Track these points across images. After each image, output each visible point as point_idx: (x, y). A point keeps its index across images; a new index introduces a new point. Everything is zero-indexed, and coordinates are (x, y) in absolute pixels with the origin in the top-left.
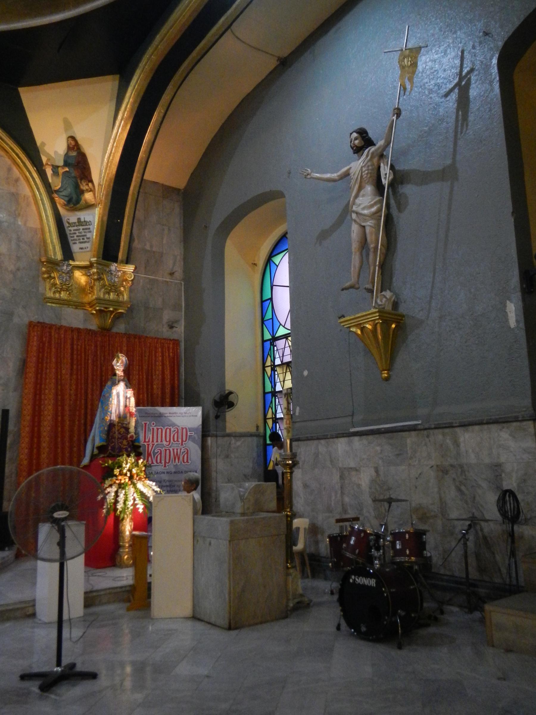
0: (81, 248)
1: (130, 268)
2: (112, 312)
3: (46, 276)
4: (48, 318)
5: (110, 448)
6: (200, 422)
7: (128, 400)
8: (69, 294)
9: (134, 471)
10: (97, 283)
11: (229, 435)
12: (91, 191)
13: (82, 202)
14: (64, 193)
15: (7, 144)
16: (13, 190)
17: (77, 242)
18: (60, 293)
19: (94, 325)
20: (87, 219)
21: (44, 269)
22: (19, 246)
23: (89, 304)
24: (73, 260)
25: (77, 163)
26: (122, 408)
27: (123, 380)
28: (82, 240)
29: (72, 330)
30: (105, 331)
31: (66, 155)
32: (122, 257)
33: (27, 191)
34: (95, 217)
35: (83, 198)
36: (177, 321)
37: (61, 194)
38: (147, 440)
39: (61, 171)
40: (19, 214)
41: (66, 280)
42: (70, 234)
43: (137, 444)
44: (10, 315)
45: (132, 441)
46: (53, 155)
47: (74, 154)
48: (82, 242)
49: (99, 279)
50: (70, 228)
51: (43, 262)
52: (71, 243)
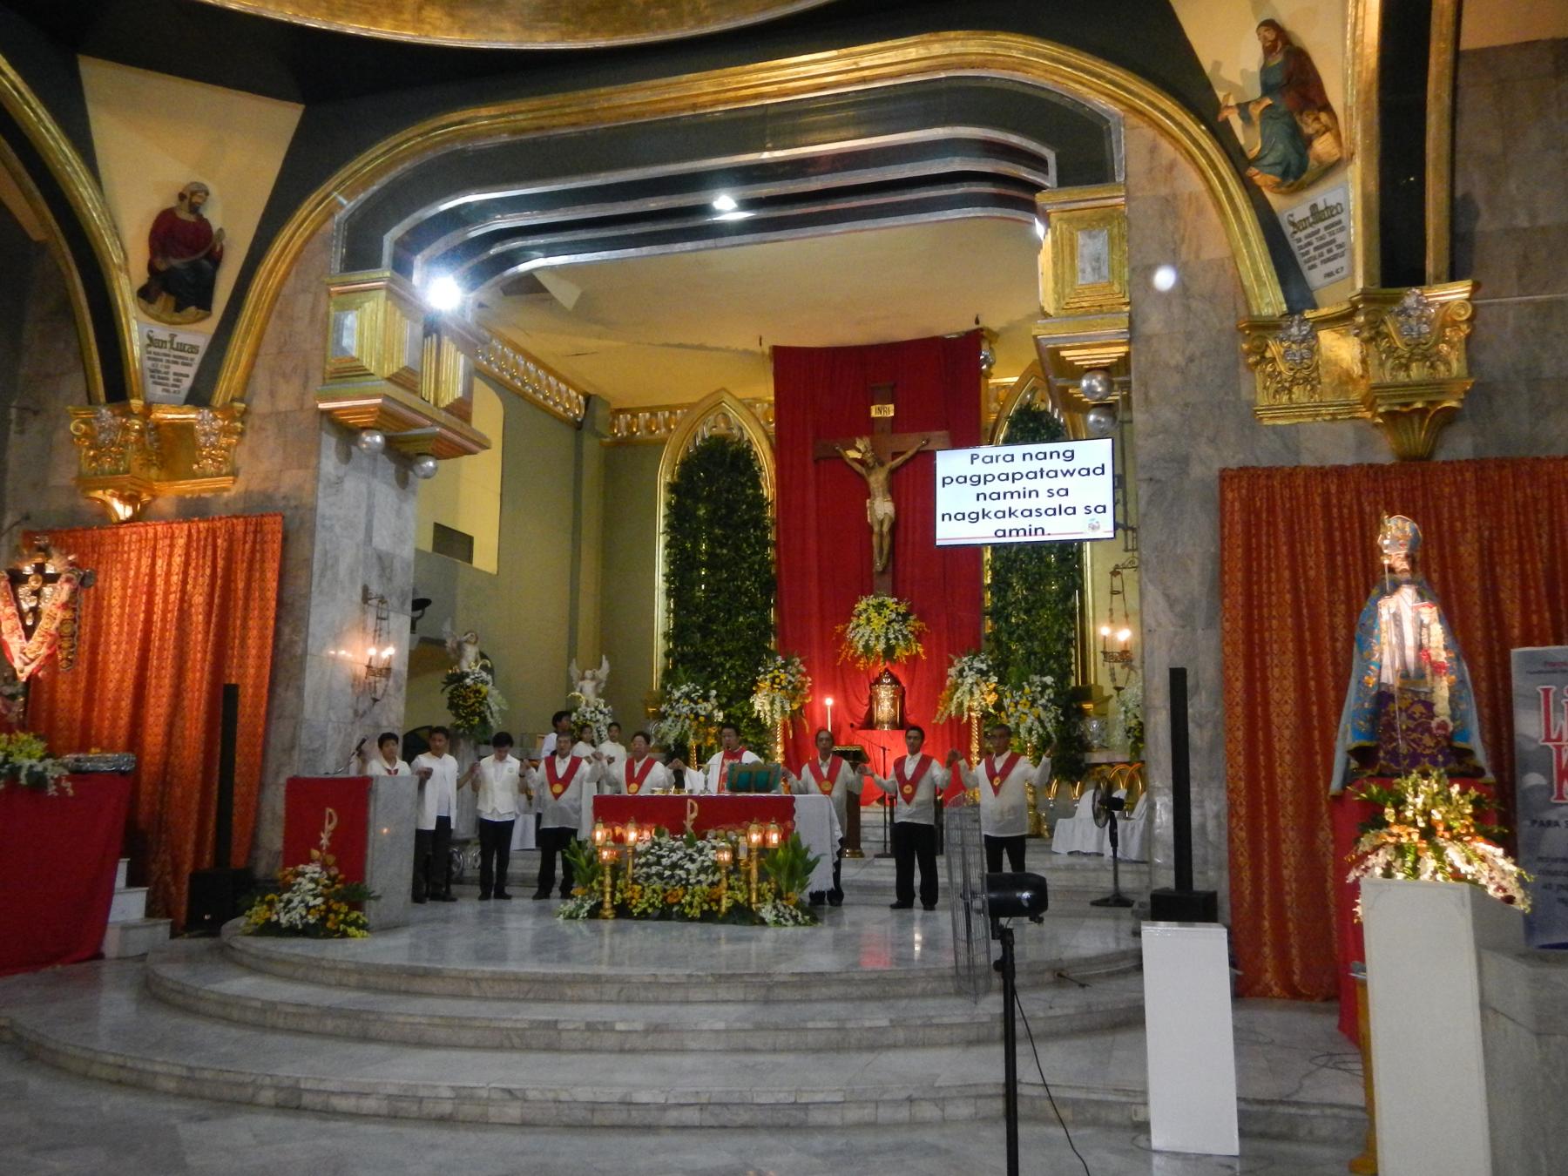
0: (1329, 275)
1: (1457, 293)
2: (1423, 412)
3: (1252, 360)
4: (1265, 455)
5: (1381, 754)
7: (1424, 631)
8: (1313, 389)
9: (1437, 815)
12: (1327, 130)
13: (1312, 163)
14: (1270, 159)
15: (1141, 98)
16: (1164, 191)
17: (1317, 262)
19: (1383, 452)
20: (1332, 202)
21: (1245, 346)
22: (1188, 308)
24: (1315, 307)
25: (1293, 77)
26: (1410, 654)
27: (1408, 582)
28: (1327, 256)
29: (1323, 473)
31: (1265, 71)
32: (1436, 267)
33: (1197, 184)
34: (1351, 191)
35: (1312, 154)
37: (1265, 162)
38: (1554, 736)
39: (1255, 111)
40: (1183, 239)
42: (1301, 248)
43: (1458, 744)
44: (1183, 462)
45: (1445, 737)
46: (1240, 83)
47: (1278, 59)
48: (1329, 260)
50: (1301, 235)
51: (1242, 330)
52: (1304, 267)
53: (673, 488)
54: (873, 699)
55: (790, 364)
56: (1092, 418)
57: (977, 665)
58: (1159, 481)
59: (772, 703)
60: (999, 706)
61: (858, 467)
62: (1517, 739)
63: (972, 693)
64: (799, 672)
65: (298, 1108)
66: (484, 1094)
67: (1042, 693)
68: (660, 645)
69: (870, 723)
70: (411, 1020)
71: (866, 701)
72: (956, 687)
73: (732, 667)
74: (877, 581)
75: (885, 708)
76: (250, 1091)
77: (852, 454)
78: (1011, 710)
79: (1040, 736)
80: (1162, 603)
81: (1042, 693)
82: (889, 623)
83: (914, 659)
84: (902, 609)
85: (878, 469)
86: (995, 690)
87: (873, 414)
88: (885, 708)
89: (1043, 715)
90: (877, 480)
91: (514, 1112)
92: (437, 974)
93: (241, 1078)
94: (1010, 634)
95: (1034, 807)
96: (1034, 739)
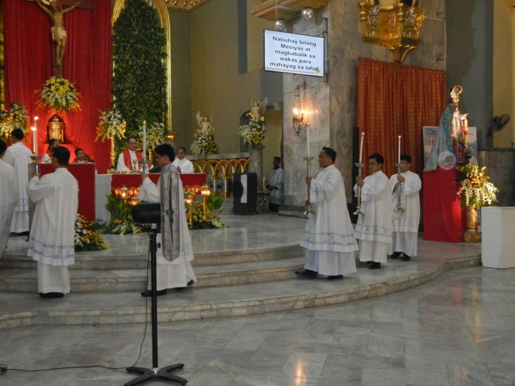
2: (408, 48)
6: (476, 140)
10: (400, 24)
11: (497, 150)
18: (372, 33)
19: (391, 59)
21: (362, 13)
23: (390, 41)
30: (399, 62)
36: (441, 55)
41: (375, 22)
43: (469, 155)
44: (342, 52)
49: (403, 21)
54: (49, 128)
56: (278, 23)
58: (336, 57)
61: (45, 9)
62: (425, 154)
65: (314, 306)
66: (378, 285)
70: (272, 271)
71: (46, 129)
72: (107, 126)
74: (55, 70)
76: (291, 304)
80: (336, 102)
84: (72, 86)
85: (58, 13)
89: (161, 140)
90: (58, 18)
91: (384, 291)
92: (240, 253)
93: (290, 299)
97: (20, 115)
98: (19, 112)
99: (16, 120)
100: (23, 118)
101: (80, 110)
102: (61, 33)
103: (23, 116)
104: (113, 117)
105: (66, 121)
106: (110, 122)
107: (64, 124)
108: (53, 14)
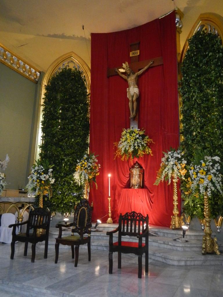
53: (47, 88)
54: (131, 176)
55: (98, 41)
57: (176, 155)
59: (81, 175)
60: (187, 176)
61: (123, 76)
63: (173, 170)
64: (94, 162)
67: (213, 166)
68: (39, 151)
69: (129, 185)
71: (128, 176)
73: (68, 161)
75: (136, 180)
77: (122, 70)
78: (194, 176)
79: (212, 192)
81: (213, 166)
82: (135, 139)
83: (146, 156)
84: (141, 133)
86: (185, 167)
87: (131, 55)
88: (136, 180)
89: (214, 179)
90: (131, 80)
94: (193, 140)
95: (210, 235)
96: (209, 194)
97: (85, 163)
98: (86, 161)
99: (82, 168)
100: (89, 166)
101: (152, 155)
102: (133, 91)
103: (91, 165)
104: (170, 157)
105: (144, 168)
106: (167, 163)
107: (144, 170)
108: (128, 78)
